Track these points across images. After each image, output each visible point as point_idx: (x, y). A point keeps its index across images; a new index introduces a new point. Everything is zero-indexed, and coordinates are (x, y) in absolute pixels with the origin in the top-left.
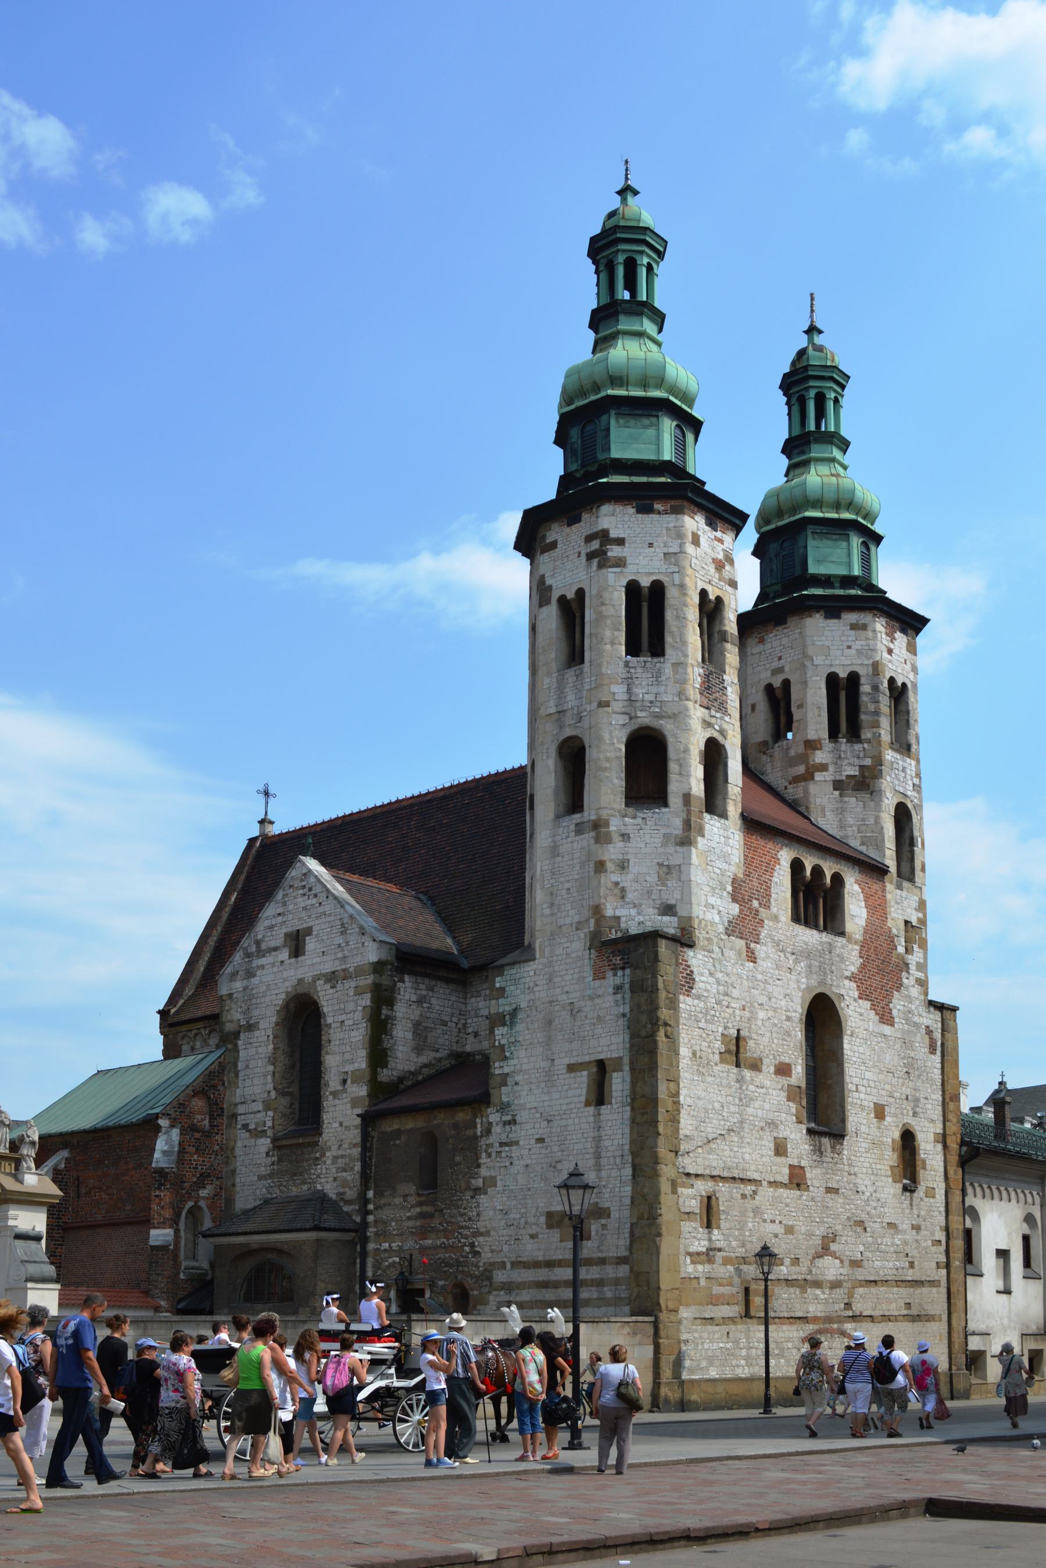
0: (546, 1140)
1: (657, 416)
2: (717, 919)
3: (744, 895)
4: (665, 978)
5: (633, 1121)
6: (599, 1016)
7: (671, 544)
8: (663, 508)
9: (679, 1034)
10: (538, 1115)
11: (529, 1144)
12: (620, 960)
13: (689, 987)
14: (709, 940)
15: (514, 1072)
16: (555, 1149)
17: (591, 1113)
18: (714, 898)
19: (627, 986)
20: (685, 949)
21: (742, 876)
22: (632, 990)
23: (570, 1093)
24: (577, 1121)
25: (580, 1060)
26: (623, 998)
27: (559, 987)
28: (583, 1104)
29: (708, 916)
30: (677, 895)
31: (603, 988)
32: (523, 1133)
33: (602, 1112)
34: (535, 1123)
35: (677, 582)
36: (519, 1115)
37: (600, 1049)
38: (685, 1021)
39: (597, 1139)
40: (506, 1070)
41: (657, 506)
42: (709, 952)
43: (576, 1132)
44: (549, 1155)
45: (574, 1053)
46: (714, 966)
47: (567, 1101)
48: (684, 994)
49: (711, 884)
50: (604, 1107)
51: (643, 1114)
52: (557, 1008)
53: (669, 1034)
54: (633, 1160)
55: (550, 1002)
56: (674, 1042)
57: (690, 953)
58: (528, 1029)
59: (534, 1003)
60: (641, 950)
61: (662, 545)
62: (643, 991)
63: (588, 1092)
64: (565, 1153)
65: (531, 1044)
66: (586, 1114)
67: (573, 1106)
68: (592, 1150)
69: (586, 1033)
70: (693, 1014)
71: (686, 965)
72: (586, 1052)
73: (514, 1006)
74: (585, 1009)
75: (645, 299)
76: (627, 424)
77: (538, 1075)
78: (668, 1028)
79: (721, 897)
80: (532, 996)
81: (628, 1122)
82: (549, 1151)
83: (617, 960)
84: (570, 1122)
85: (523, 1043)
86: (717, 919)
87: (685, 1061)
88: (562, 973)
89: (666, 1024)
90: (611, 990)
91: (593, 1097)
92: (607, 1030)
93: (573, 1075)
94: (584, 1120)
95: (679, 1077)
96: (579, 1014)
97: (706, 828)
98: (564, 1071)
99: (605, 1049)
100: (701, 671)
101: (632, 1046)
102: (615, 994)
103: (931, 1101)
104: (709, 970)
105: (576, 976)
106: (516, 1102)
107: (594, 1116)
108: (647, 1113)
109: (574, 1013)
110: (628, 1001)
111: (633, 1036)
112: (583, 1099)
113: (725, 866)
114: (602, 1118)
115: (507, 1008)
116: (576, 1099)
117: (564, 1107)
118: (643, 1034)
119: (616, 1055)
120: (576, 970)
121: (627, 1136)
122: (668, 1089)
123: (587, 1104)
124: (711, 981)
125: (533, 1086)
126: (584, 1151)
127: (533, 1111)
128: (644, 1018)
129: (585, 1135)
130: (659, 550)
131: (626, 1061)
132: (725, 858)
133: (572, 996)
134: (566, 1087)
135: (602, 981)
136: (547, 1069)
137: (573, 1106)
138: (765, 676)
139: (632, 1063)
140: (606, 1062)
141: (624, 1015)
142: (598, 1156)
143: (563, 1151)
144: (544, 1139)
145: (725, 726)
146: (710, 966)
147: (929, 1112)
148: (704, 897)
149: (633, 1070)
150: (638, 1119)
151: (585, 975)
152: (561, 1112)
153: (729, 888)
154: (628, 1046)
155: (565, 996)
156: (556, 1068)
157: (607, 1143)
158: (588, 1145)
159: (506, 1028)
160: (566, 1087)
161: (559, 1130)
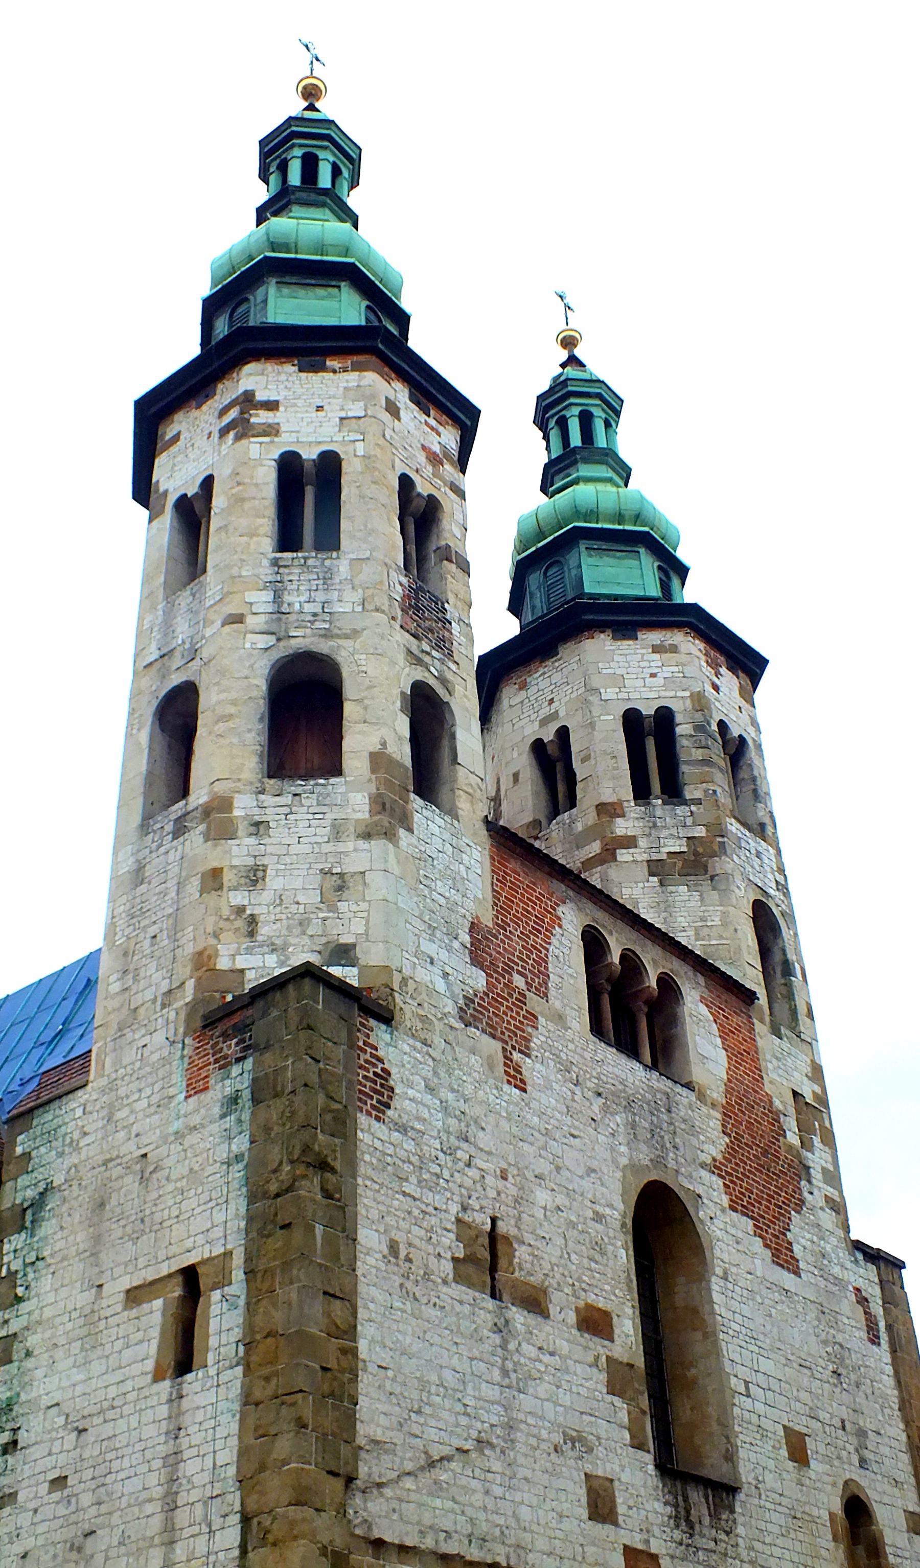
0: (70, 1482)
1: (339, 287)
2: (441, 986)
3: (496, 959)
4: (321, 1065)
5: (248, 1401)
6: (191, 1169)
7: (352, 407)
8: (340, 365)
9: (355, 1195)
10: (61, 1421)
11: (36, 1497)
12: (237, 1044)
13: (379, 1101)
14: (424, 1019)
15: (27, 1328)
16: (86, 1499)
17: (164, 1397)
18: (435, 946)
19: (246, 1095)
20: (372, 1022)
21: (490, 925)
22: (256, 1100)
23: (127, 1354)
24: (134, 1423)
25: (151, 1275)
26: (240, 1121)
27: (124, 1127)
28: (149, 1378)
29: (423, 975)
30: (358, 927)
31: (203, 1111)
32: (27, 1471)
33: (186, 1388)
34: (53, 1440)
35: (360, 452)
36: (24, 1427)
37: (189, 1243)
38: (370, 1172)
39: (171, 1460)
40: (14, 1326)
41: (330, 363)
42: (425, 1043)
43: (129, 1450)
44: (73, 1518)
45: (142, 1262)
46: (435, 1073)
47: (118, 1376)
48: (369, 1114)
49: (426, 918)
50: (189, 1377)
51: (267, 1379)
52: (117, 1172)
53: (330, 1187)
54: (242, 1504)
55: (105, 1163)
56: (342, 1209)
57: (380, 1034)
58: (62, 1228)
59: (77, 1171)
60: (275, 1013)
61: (338, 408)
62: (276, 1095)
63: (160, 1348)
64: (104, 1508)
65: (62, 1261)
66: (153, 1401)
67: (129, 1386)
68: (158, 1492)
69: (166, 1212)
70: (389, 1159)
71: (372, 1055)
72: (161, 1255)
73: (42, 1186)
74: (167, 1163)
75: (328, 185)
76: (295, 294)
77: (69, 1326)
78: (328, 1175)
79: (449, 949)
80: (75, 1160)
81: (236, 1407)
82: (73, 1508)
83: (231, 1047)
84: (122, 1424)
85: (49, 1260)
86: (441, 986)
87: (371, 1261)
88: (130, 1100)
89: (323, 1166)
90: (217, 1111)
91: (170, 1360)
92: (205, 1197)
93: (134, 1313)
94: (148, 1416)
95: (355, 1292)
96: (154, 1176)
97: (416, 819)
98: (119, 1307)
99: (200, 1239)
100: (404, 580)
101: (250, 1219)
102: (223, 1116)
103: (887, 1440)
104: (424, 1079)
105: (155, 1099)
106: (23, 1397)
107: (170, 1401)
108: (276, 1374)
109: (147, 1175)
110: (246, 1126)
111: (252, 1198)
112: (150, 1365)
113: (458, 898)
114: (185, 1403)
115: (30, 1193)
116: (137, 1369)
117: (113, 1392)
118: (273, 1188)
119: (222, 1250)
120: (157, 1087)
121: (234, 1442)
122: (328, 1314)
123: (158, 1377)
124: (429, 1103)
125: (59, 1354)
126: (145, 1495)
127: (54, 1410)
128: (275, 1153)
129: (149, 1454)
130: (333, 414)
131: (238, 1259)
132: (456, 882)
133: (144, 1140)
134: (119, 1344)
135: (202, 1096)
136: (87, 1311)
137: (129, 1386)
138: (531, 730)
139: (248, 1259)
140: (201, 1270)
141: (238, 1158)
142: (170, 1506)
143: (99, 1503)
144: (66, 1477)
145: (449, 676)
146: (427, 1071)
147: (886, 1461)
148: (413, 938)
149: (250, 1273)
150: (258, 1394)
151: (172, 1091)
152: (106, 1404)
153: (466, 939)
154: (243, 1224)
155: (131, 1146)
156: (104, 1303)
157: (190, 1467)
158: (153, 1480)
159: (23, 1235)
160: (119, 1344)
161: (96, 1452)
